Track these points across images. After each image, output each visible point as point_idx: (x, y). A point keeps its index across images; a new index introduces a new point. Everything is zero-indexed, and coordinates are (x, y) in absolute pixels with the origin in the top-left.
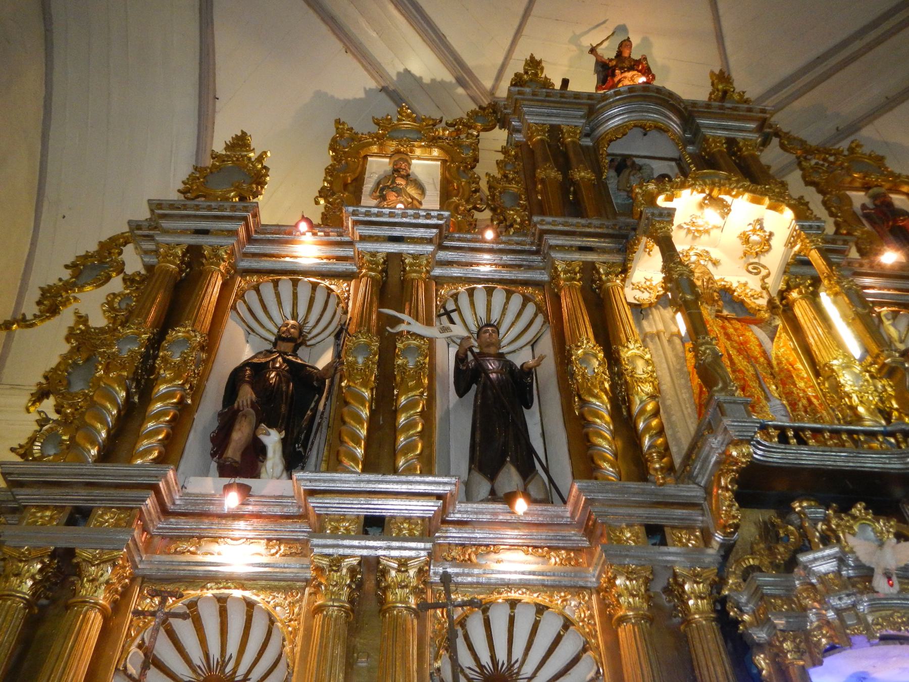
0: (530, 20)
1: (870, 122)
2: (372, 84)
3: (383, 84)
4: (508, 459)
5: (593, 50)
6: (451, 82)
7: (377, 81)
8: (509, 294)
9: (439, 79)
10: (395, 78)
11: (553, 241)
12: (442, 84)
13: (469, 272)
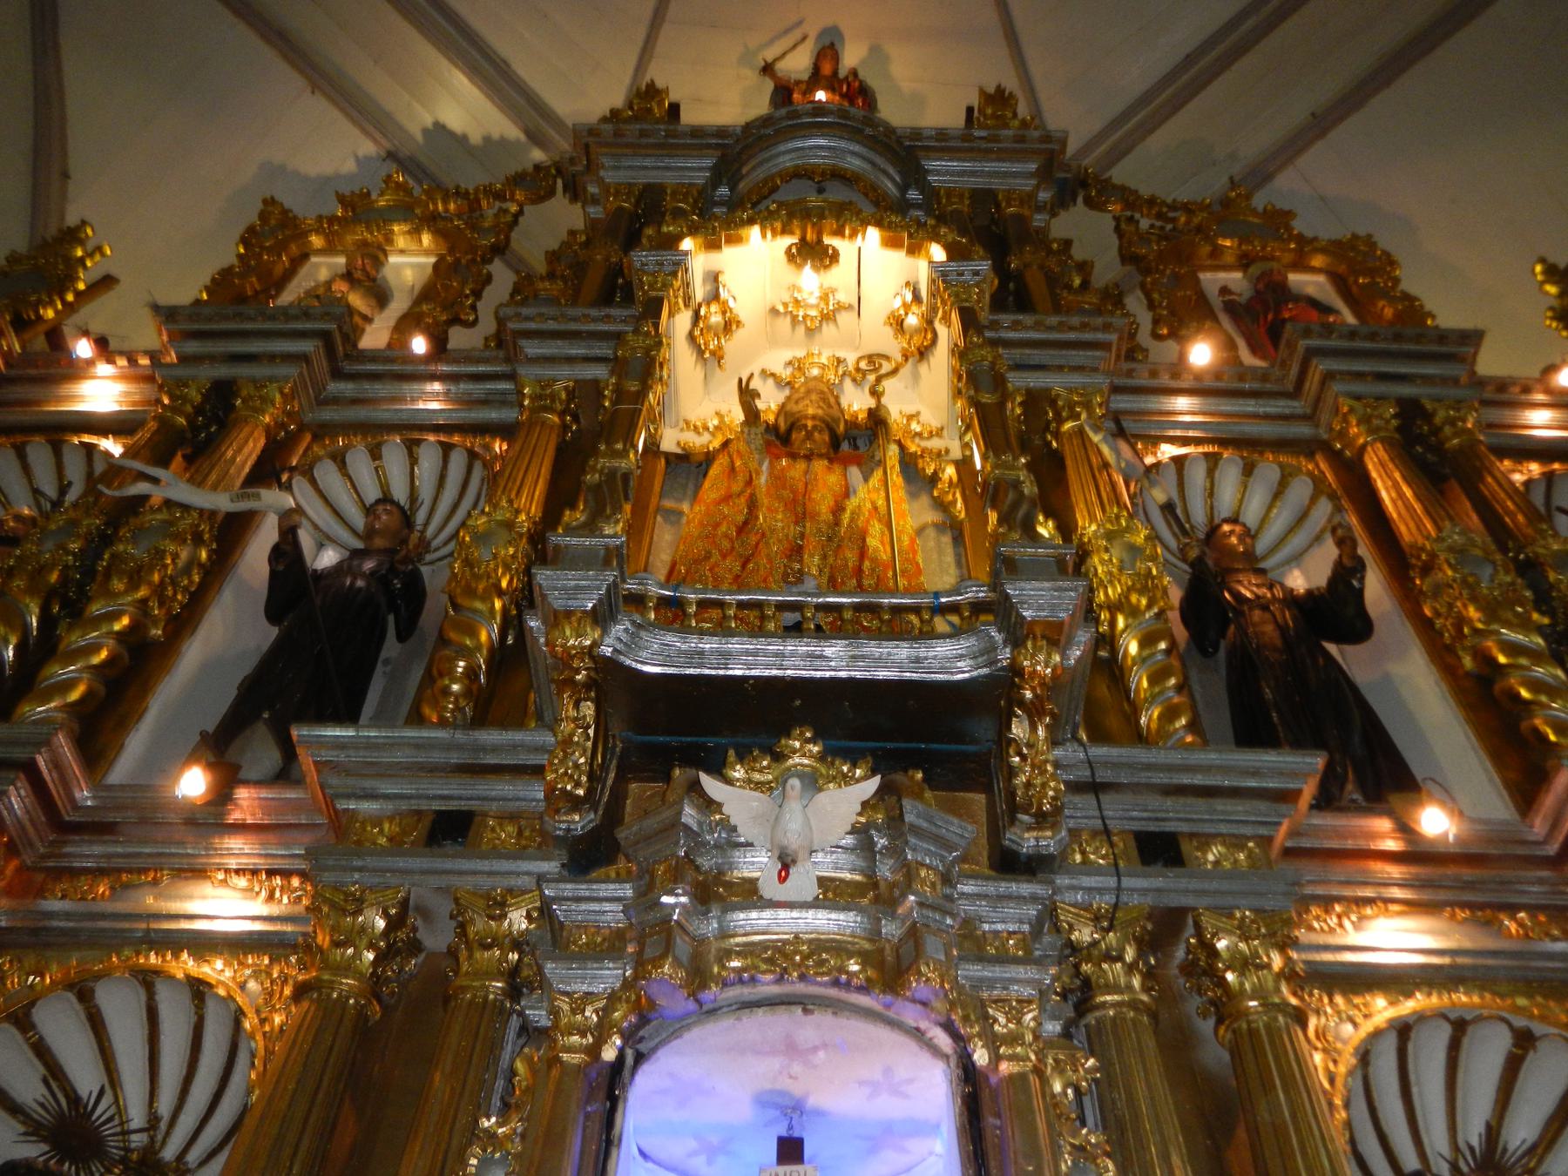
0: (666, 31)
1: (1290, 160)
2: (368, 148)
3: (388, 145)
4: (266, 715)
5: (767, 69)
6: (518, 141)
7: (375, 141)
8: (447, 449)
9: (496, 136)
10: (419, 137)
11: (532, 348)
12: (503, 142)
13: (382, 413)
